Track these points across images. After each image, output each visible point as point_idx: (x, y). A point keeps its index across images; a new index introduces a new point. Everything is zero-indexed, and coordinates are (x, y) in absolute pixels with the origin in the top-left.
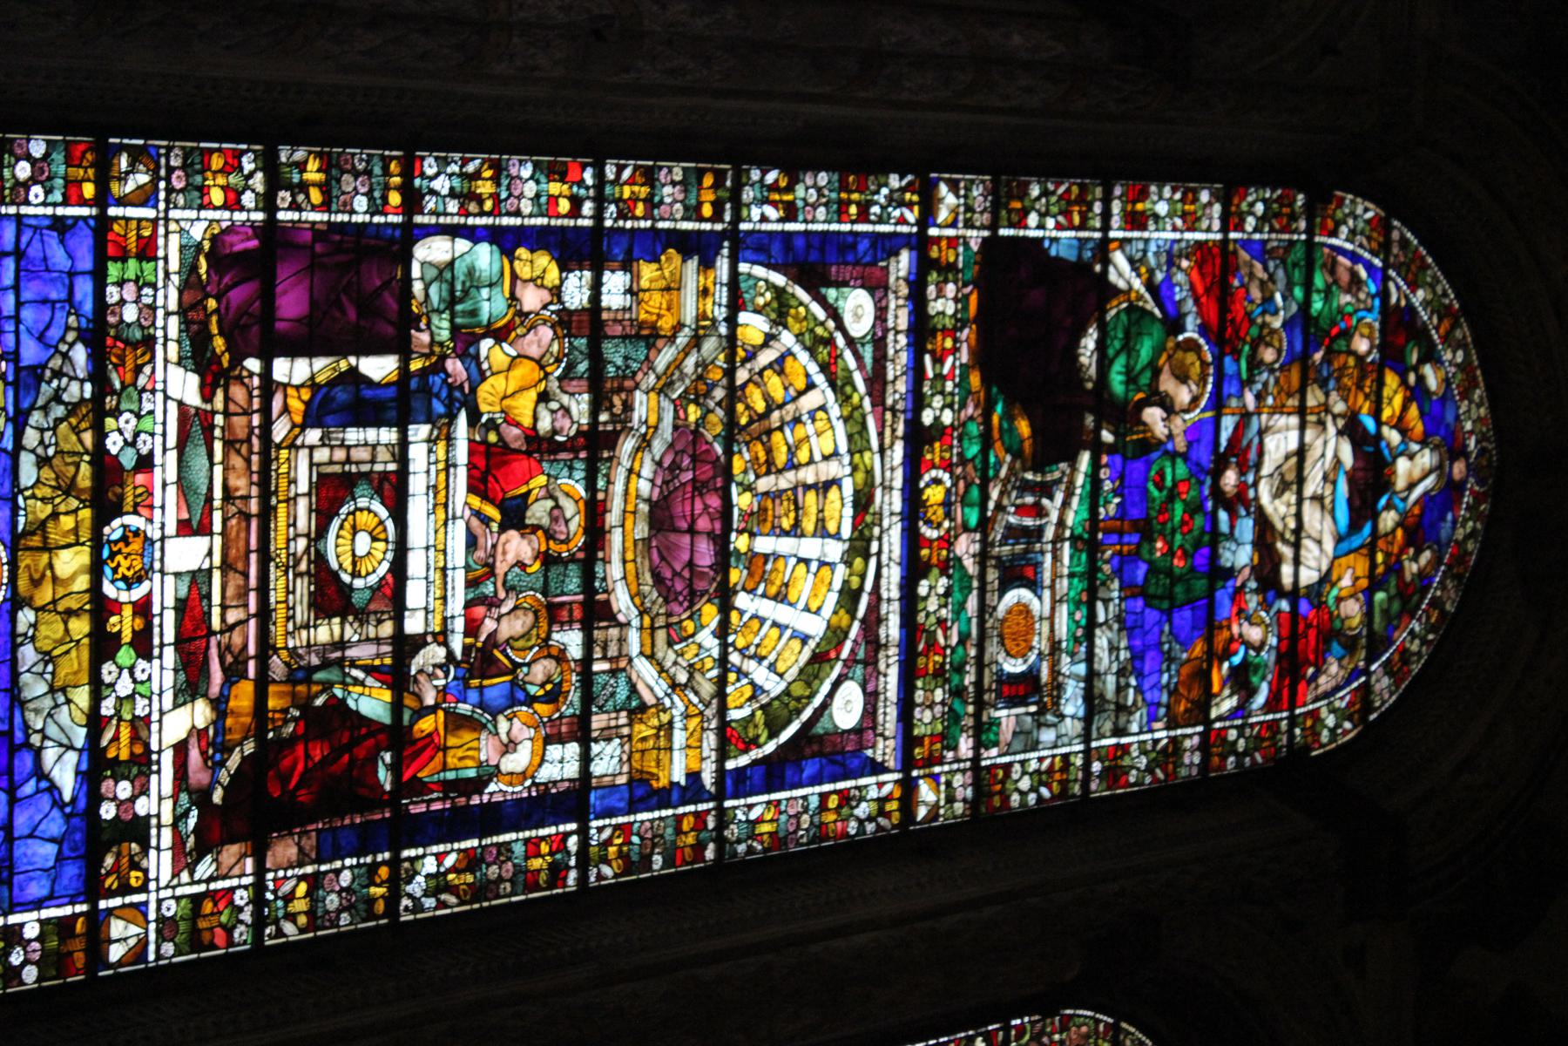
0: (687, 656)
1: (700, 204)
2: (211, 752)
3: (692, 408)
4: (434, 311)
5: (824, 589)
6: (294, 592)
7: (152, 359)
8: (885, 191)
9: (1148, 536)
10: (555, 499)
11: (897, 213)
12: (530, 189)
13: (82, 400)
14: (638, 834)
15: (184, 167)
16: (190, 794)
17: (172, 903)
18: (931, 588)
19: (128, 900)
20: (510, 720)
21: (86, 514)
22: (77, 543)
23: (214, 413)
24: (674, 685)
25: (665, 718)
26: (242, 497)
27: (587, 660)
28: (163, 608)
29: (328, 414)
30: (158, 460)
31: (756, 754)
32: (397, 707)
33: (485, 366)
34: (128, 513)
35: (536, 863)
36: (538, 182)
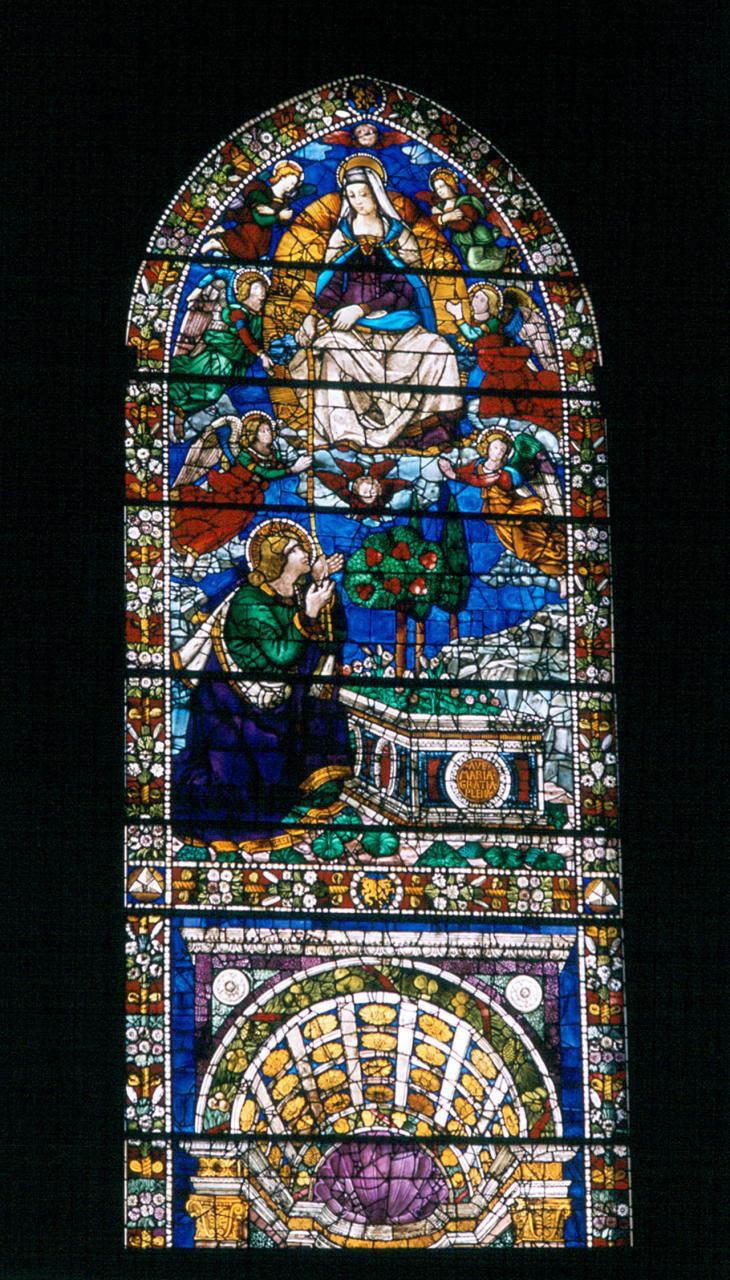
3: (301, 1182)
5: (437, 1023)
8: (139, 959)
9: (406, 608)
11: (155, 943)
14: (601, 1231)
18: (441, 895)
24: (498, 1195)
31: (553, 1103)
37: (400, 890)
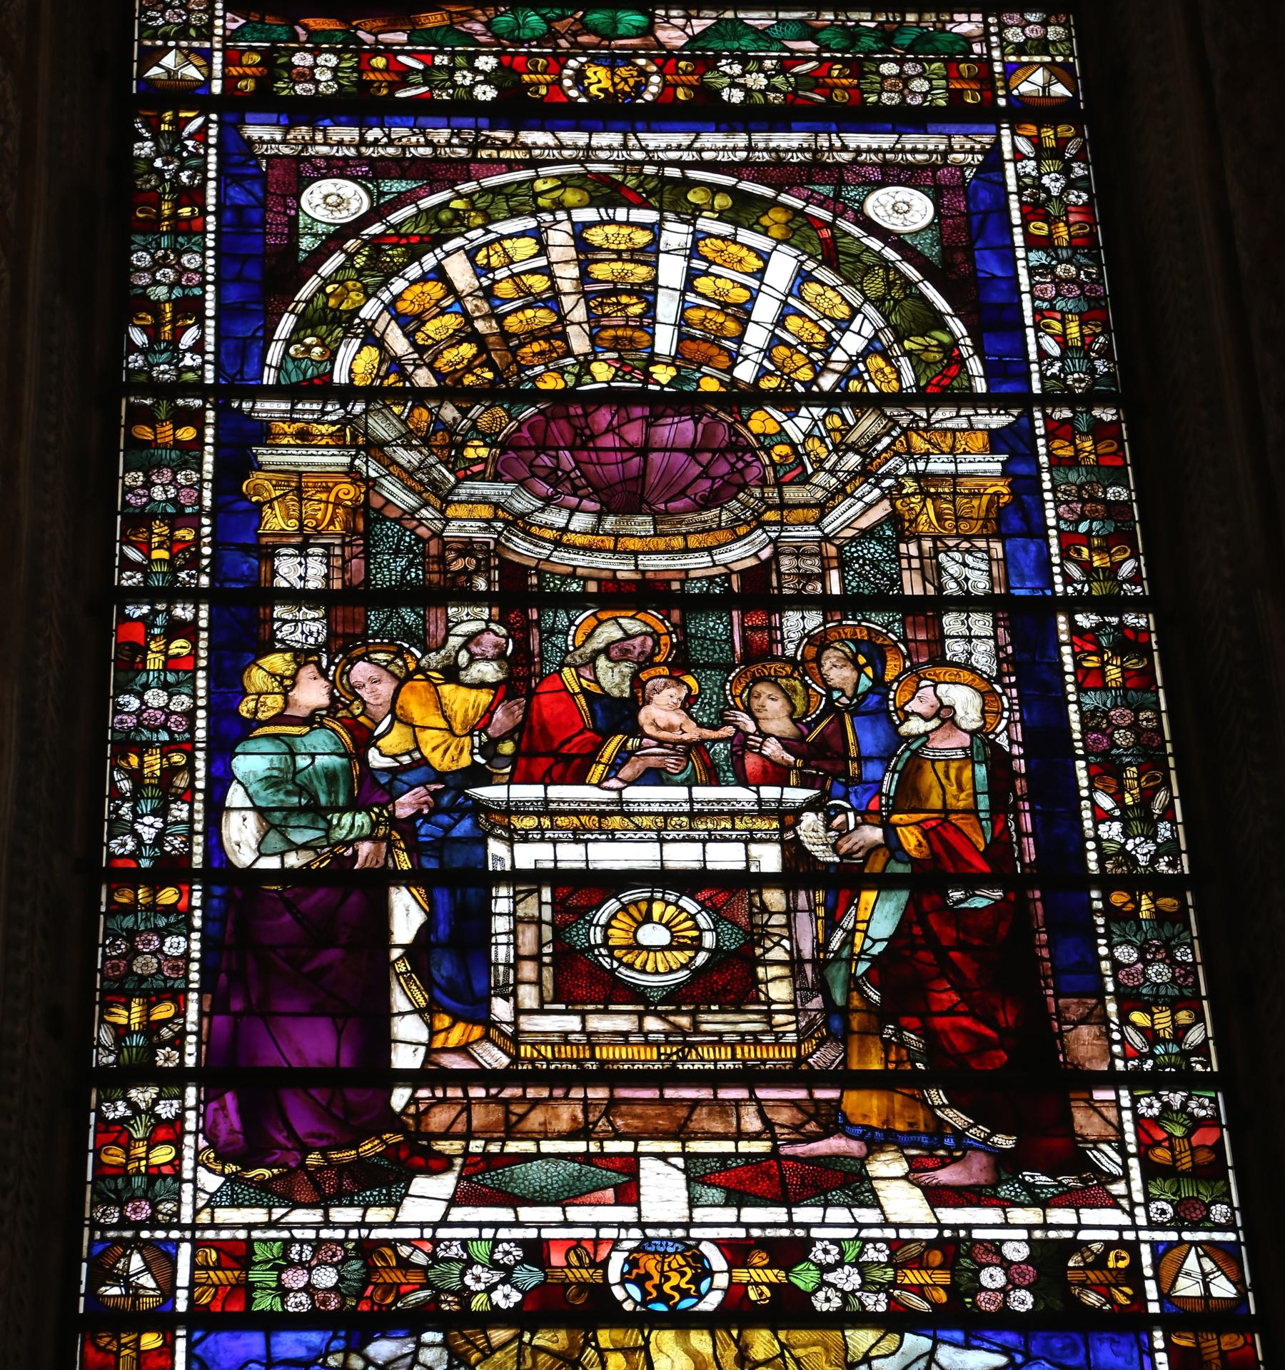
0: (823, 453)
1: (178, 444)
2: (942, 1152)
3: (470, 453)
4: (327, 837)
5: (733, 249)
6: (720, 1034)
7: (391, 1244)
8: (158, 163)
10: (597, 653)
12: (156, 698)
13: (444, 1344)
14: (1077, 523)
15: (121, 1205)
16: (999, 1182)
17: (1153, 1206)
18: (733, 85)
19: (1148, 1272)
20: (907, 716)
21: (604, 1337)
22: (646, 1348)
23: (466, 1154)
24: (864, 473)
25: (910, 486)
26: (586, 1112)
27: (825, 603)
28: (738, 1224)
29: (470, 987)
30: (531, 1233)
32: (884, 883)
33: (406, 760)
34: (605, 1276)
35: (1113, 673)
36: (146, 687)
37: (655, 79)
